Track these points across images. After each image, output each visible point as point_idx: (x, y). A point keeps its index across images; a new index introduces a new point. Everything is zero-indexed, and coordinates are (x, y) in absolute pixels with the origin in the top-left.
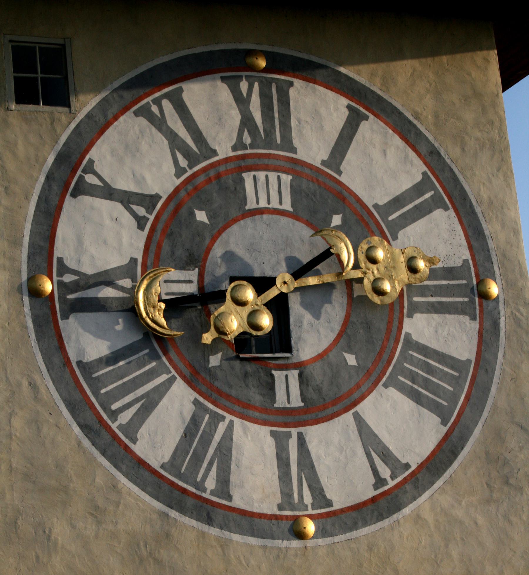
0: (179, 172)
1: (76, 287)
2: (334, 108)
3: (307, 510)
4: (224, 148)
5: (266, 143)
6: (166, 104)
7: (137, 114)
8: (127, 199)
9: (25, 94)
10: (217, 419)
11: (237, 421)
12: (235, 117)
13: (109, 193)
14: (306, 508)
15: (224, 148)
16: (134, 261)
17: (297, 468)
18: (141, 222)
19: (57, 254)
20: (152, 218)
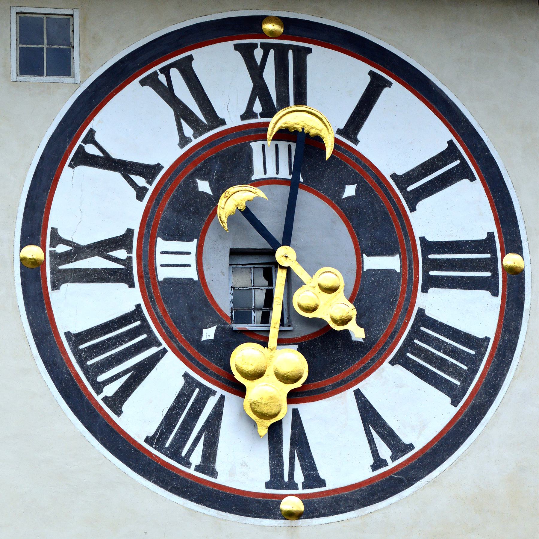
0: (184, 140)
1: (67, 257)
2: (357, 74)
3: (297, 489)
6: (174, 73)
7: (143, 83)
8: (126, 168)
9: (29, 64)
10: (206, 393)
12: (247, 85)
13: (107, 162)
14: (296, 487)
15: (233, 119)
16: (130, 232)
18: (140, 193)
19: (52, 223)
20: (151, 188)
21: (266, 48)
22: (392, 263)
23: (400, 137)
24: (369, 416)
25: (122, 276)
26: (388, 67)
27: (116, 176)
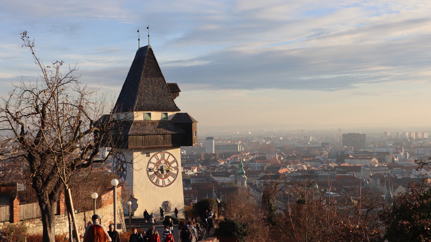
2: (168, 155)
4: (160, 159)
5: (163, 158)
8: (153, 163)
9: (147, 156)
15: (160, 159)
17: (164, 182)
23: (171, 159)
24: (169, 180)
26: (170, 154)
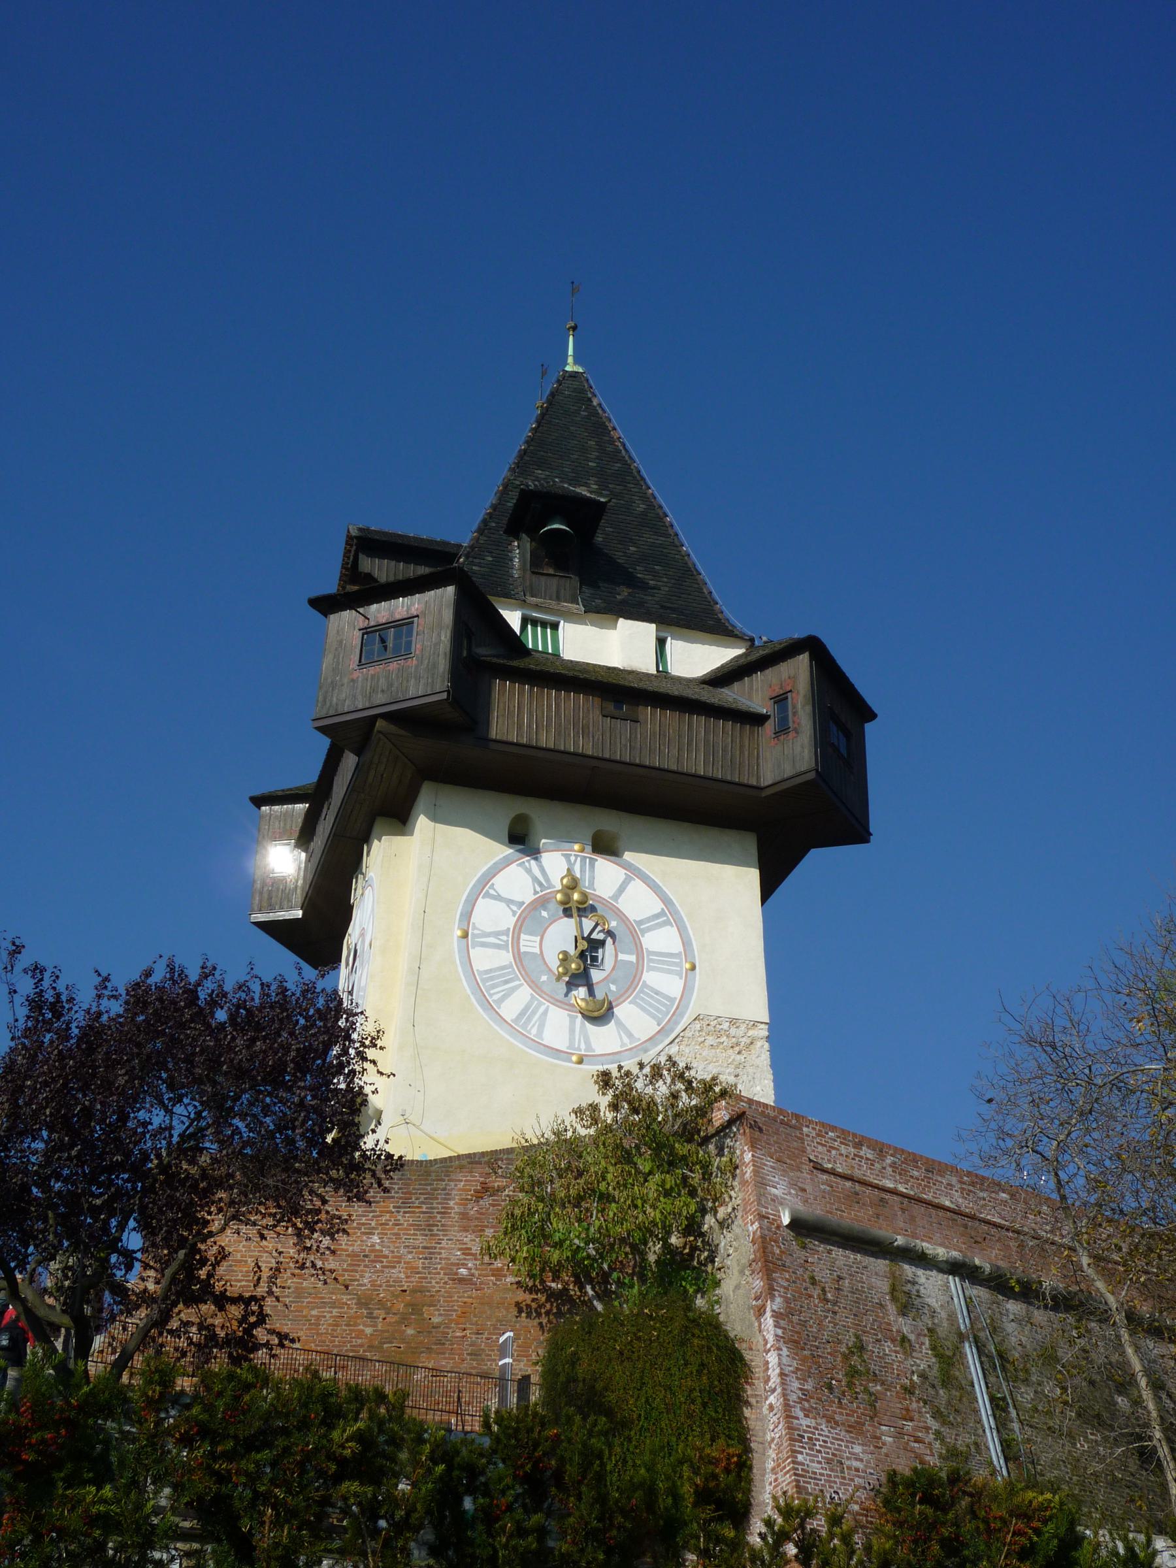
0: (536, 893)
10: (540, 1004)
11: (552, 1007)
18: (514, 913)
21: (576, 856)
22: (633, 958)
25: (504, 947)
27: (503, 905)
